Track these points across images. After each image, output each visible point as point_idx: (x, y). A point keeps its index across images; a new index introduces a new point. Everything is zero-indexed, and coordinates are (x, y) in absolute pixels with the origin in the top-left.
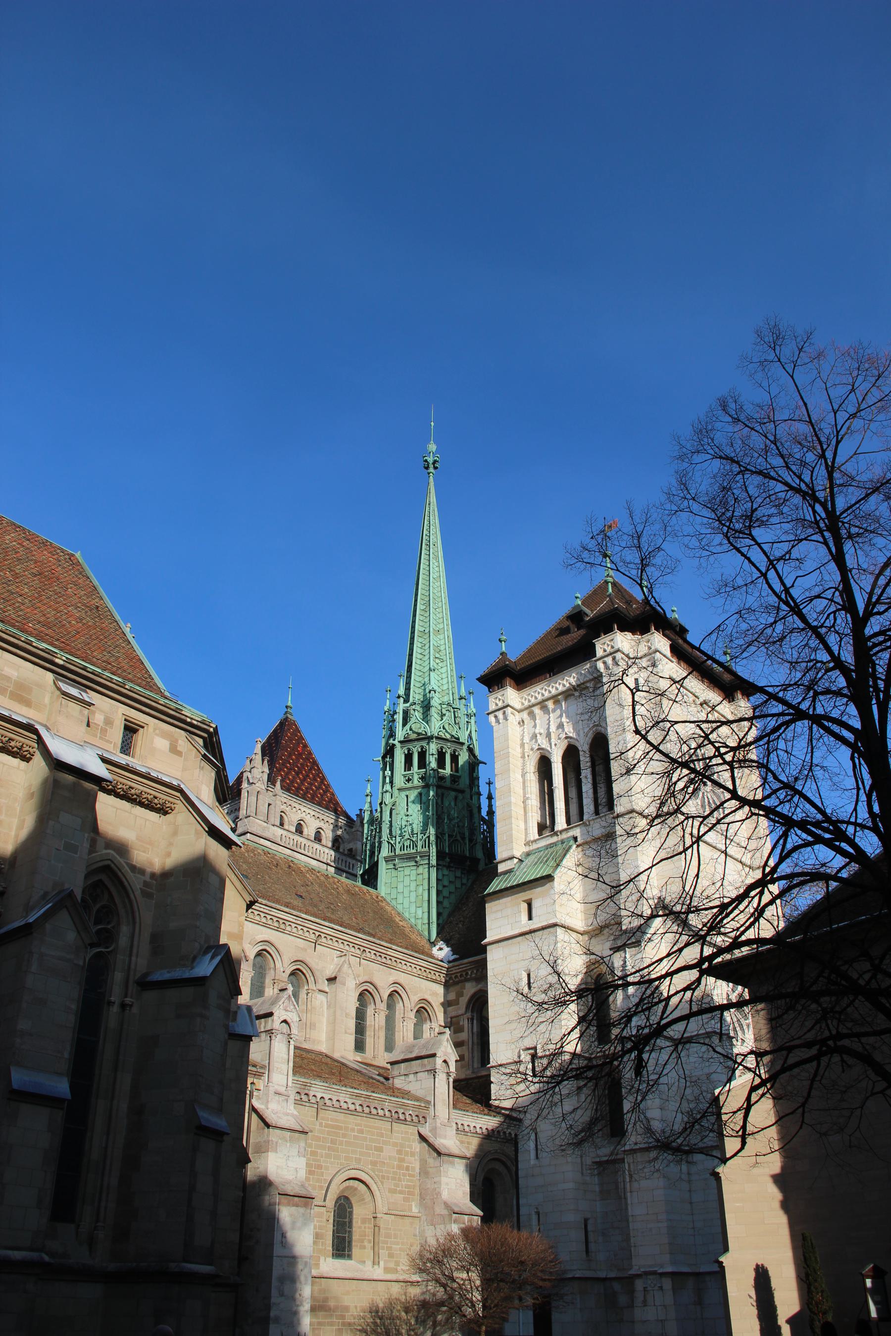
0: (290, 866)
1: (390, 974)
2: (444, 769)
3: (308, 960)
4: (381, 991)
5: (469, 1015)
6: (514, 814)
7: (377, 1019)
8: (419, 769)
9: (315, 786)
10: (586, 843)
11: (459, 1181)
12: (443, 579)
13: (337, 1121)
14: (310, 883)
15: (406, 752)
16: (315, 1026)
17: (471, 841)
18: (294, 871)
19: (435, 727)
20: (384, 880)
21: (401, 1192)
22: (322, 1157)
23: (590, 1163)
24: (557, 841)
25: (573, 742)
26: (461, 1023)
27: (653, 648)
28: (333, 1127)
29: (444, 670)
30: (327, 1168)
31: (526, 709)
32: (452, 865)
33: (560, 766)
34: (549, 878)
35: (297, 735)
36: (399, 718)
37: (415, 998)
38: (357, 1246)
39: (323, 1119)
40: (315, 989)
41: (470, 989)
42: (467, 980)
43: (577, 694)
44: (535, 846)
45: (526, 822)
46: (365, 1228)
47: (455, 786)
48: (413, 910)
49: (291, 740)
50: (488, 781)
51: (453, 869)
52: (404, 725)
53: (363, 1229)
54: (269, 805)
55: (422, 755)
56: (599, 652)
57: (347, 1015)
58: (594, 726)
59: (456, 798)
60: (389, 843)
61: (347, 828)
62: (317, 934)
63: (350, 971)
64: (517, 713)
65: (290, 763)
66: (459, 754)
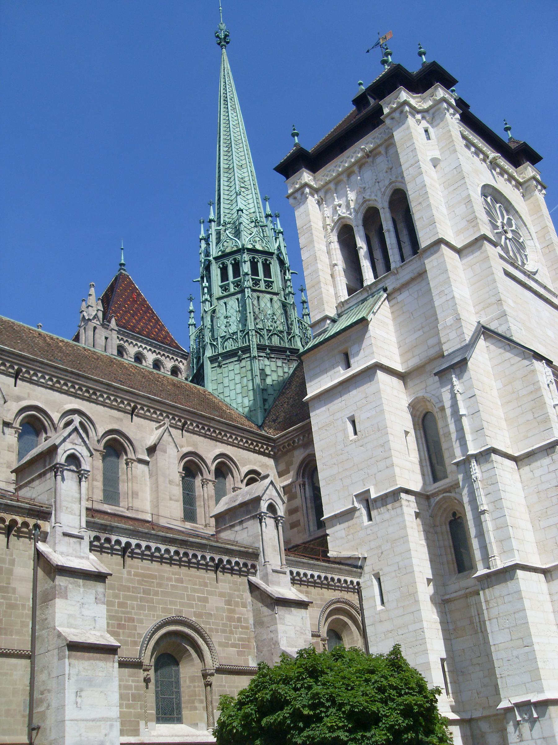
0: (112, 361)
1: (216, 446)
2: (258, 276)
3: (124, 430)
4: (209, 462)
5: (300, 480)
6: (322, 279)
7: (205, 488)
8: (234, 278)
9: (151, 326)
10: (395, 290)
11: (298, 628)
12: (242, 126)
13: (148, 569)
14: (132, 374)
15: (221, 266)
16: (137, 494)
17: (289, 334)
18: (116, 365)
19: (246, 241)
20: (210, 379)
21: (234, 646)
22: (133, 608)
23: (440, 602)
24: (368, 297)
25: (371, 204)
26: (294, 491)
27: (438, 98)
28: (144, 575)
29: (249, 197)
30: (141, 621)
31: (323, 186)
32: (273, 356)
33: (361, 228)
34: (363, 322)
35: (131, 286)
36: (213, 238)
37: (244, 470)
38: (187, 707)
39: (131, 567)
40: (134, 458)
41: (299, 456)
42: (294, 448)
43: (370, 160)
44: (346, 307)
45: (335, 286)
46: (194, 687)
47: (269, 290)
48: (239, 400)
49: (125, 290)
50: (300, 288)
51: (274, 360)
52: (217, 243)
53: (192, 688)
54: (106, 338)
55: (237, 267)
56: (386, 111)
57: (171, 482)
58: (390, 184)
59: (271, 300)
60: (211, 344)
61: (183, 360)
62: (132, 405)
63: (170, 439)
64: (313, 192)
65: (125, 307)
66: (270, 263)
